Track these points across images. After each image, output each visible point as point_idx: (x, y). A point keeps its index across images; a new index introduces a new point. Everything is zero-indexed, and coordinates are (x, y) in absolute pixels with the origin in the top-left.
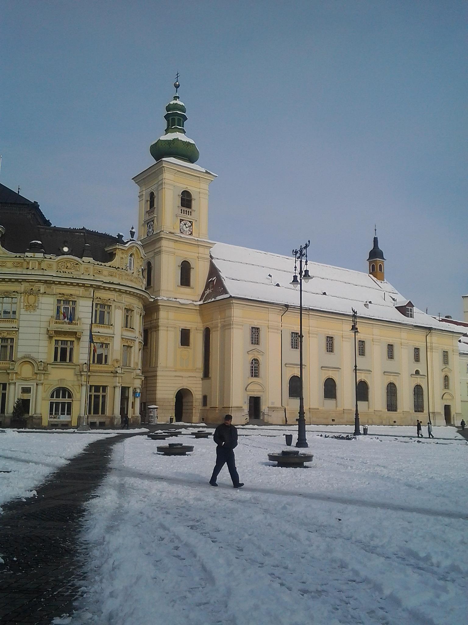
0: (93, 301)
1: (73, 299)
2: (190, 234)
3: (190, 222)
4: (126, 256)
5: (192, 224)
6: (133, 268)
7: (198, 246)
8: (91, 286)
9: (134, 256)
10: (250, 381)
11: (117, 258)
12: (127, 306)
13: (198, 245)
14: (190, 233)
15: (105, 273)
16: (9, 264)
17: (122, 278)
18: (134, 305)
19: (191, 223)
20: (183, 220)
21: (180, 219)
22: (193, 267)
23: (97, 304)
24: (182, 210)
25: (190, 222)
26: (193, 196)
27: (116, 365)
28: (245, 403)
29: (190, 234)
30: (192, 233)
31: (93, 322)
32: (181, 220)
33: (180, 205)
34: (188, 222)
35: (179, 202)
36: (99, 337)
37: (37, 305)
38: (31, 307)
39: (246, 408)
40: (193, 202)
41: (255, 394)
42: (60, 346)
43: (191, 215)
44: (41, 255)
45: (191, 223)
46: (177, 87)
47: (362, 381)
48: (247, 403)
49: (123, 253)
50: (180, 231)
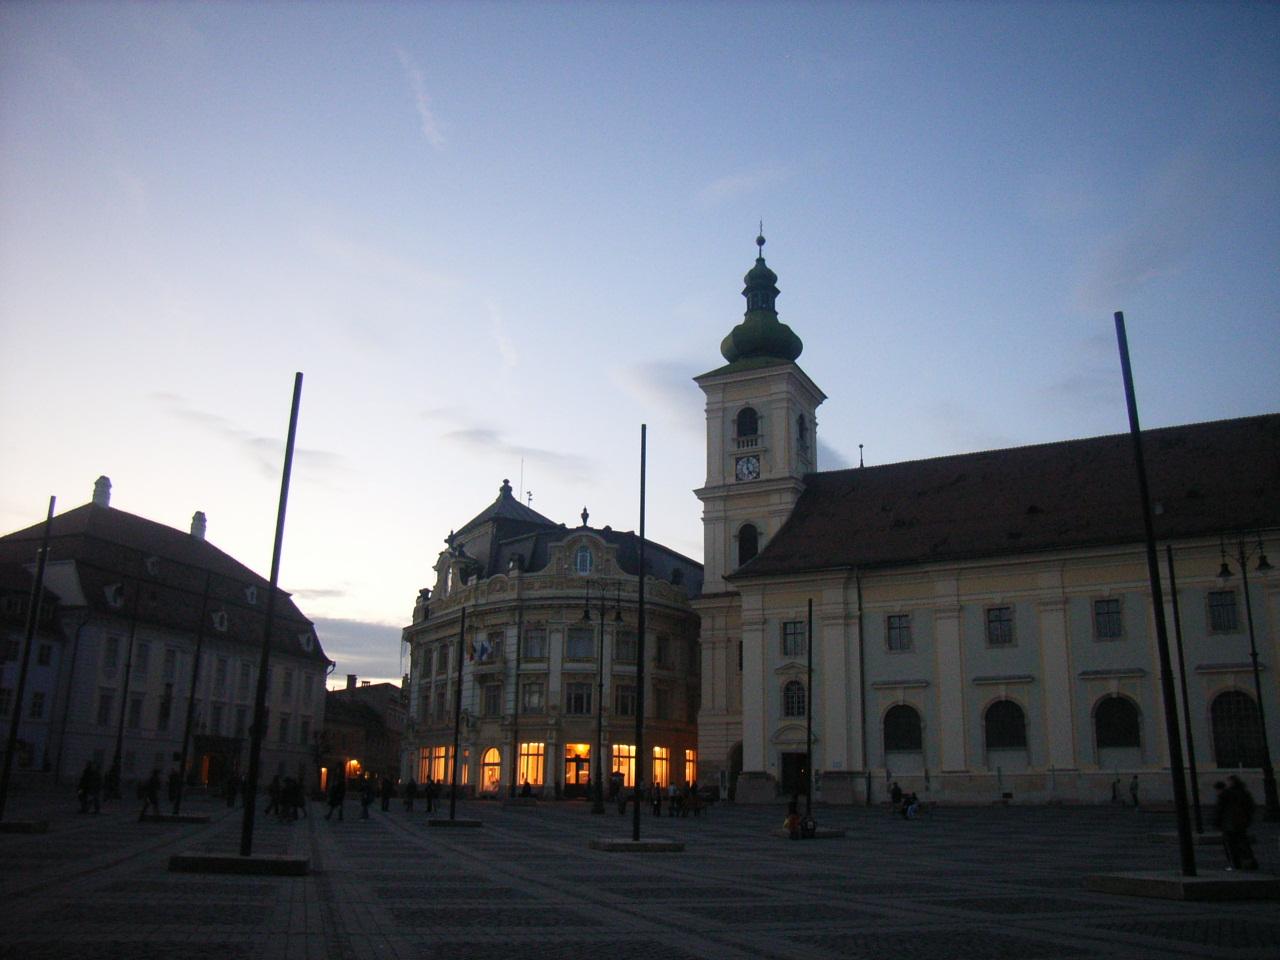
0: (519, 628)
5: (758, 460)
6: (591, 566)
7: (768, 493)
10: (783, 724)
11: (554, 560)
12: (572, 625)
15: (537, 585)
22: (763, 531)
24: (739, 443)
25: (754, 457)
26: (759, 414)
28: (773, 765)
30: (758, 474)
32: (738, 460)
33: (735, 436)
35: (732, 431)
39: (775, 772)
40: (759, 422)
46: (761, 241)
47: (1111, 698)
48: (776, 764)
49: (560, 552)
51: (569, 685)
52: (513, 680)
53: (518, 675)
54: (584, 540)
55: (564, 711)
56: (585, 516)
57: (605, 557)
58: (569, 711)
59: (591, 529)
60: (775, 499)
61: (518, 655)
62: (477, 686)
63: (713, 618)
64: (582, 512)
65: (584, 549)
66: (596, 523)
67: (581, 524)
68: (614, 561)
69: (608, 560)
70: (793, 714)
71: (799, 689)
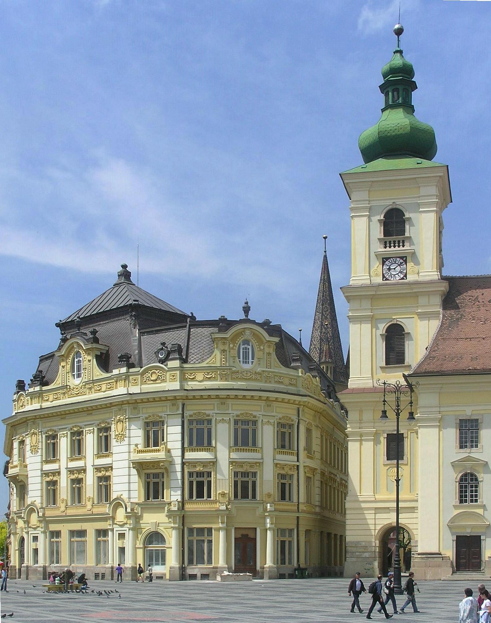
0: (183, 417)
1: (160, 418)
2: (403, 279)
3: (401, 258)
4: (231, 346)
6: (253, 359)
8: (175, 398)
9: (252, 343)
12: (237, 416)
13: (415, 292)
14: (402, 276)
16: (104, 387)
17: (226, 379)
18: (254, 413)
19: (404, 259)
20: (387, 259)
21: (383, 258)
23: (191, 422)
24: (386, 242)
25: (401, 258)
27: (221, 499)
29: (403, 279)
30: (406, 276)
31: (186, 445)
32: (384, 260)
34: (398, 259)
35: (378, 232)
36: (194, 463)
37: (125, 433)
38: (121, 437)
41: (468, 532)
42: (195, 480)
43: (403, 246)
44: (124, 370)
45: (404, 259)
49: (224, 344)
50: (384, 276)
51: (236, 474)
52: (178, 468)
53: (183, 464)
54: (248, 332)
55: (233, 498)
56: (247, 310)
57: (267, 350)
58: (236, 496)
59: (253, 322)
60: (422, 300)
61: (183, 444)
62: (134, 472)
63: (361, 411)
64: (244, 305)
65: (246, 342)
66: (256, 315)
67: (244, 317)
68: (274, 356)
69: (269, 354)
70: (466, 501)
71: (472, 480)
